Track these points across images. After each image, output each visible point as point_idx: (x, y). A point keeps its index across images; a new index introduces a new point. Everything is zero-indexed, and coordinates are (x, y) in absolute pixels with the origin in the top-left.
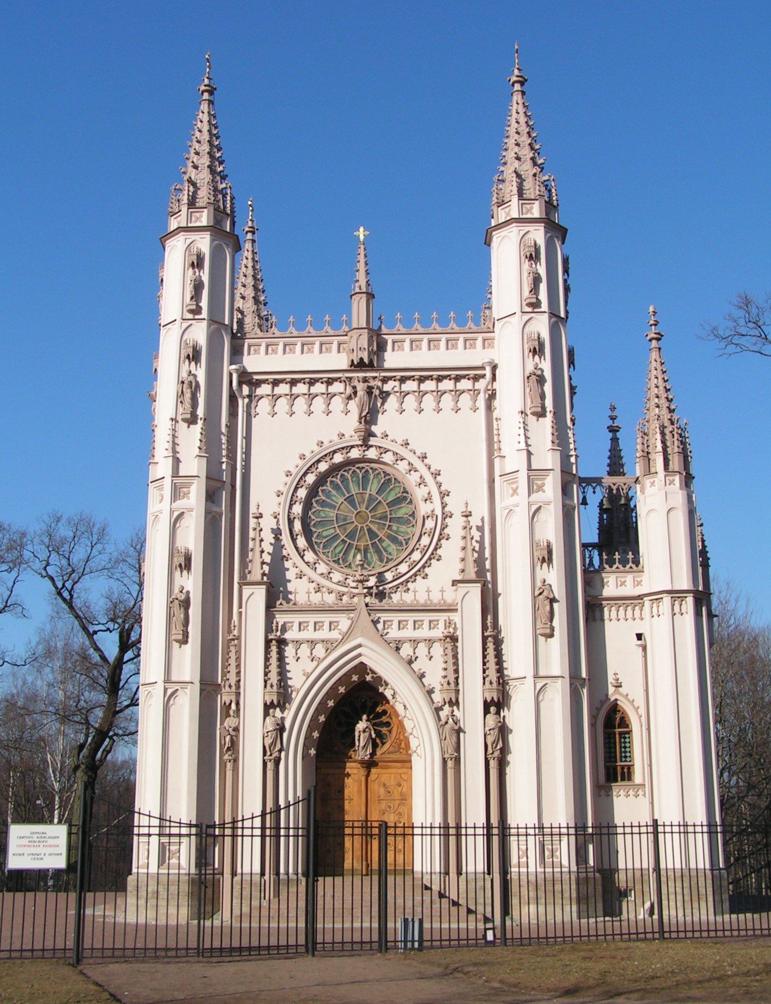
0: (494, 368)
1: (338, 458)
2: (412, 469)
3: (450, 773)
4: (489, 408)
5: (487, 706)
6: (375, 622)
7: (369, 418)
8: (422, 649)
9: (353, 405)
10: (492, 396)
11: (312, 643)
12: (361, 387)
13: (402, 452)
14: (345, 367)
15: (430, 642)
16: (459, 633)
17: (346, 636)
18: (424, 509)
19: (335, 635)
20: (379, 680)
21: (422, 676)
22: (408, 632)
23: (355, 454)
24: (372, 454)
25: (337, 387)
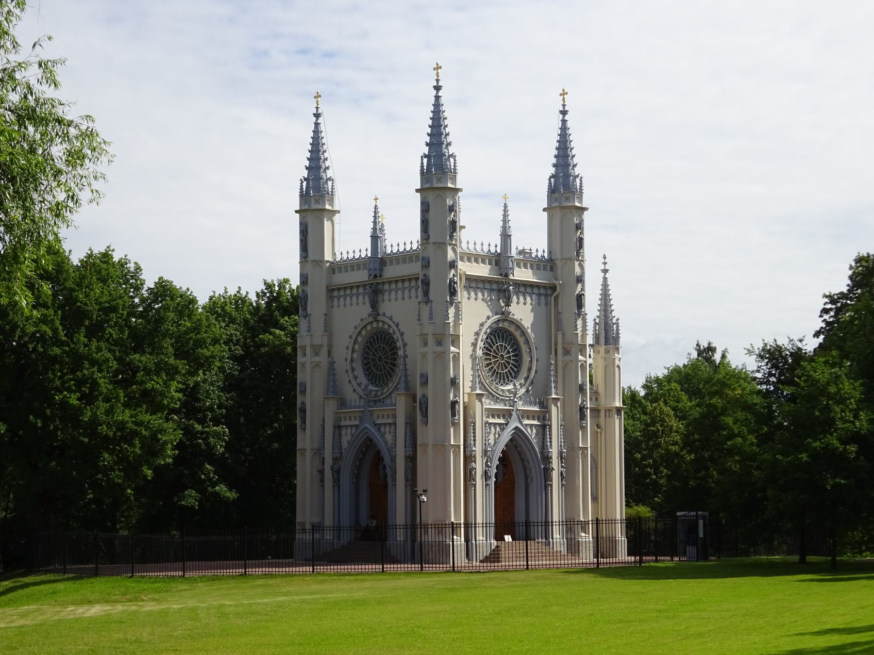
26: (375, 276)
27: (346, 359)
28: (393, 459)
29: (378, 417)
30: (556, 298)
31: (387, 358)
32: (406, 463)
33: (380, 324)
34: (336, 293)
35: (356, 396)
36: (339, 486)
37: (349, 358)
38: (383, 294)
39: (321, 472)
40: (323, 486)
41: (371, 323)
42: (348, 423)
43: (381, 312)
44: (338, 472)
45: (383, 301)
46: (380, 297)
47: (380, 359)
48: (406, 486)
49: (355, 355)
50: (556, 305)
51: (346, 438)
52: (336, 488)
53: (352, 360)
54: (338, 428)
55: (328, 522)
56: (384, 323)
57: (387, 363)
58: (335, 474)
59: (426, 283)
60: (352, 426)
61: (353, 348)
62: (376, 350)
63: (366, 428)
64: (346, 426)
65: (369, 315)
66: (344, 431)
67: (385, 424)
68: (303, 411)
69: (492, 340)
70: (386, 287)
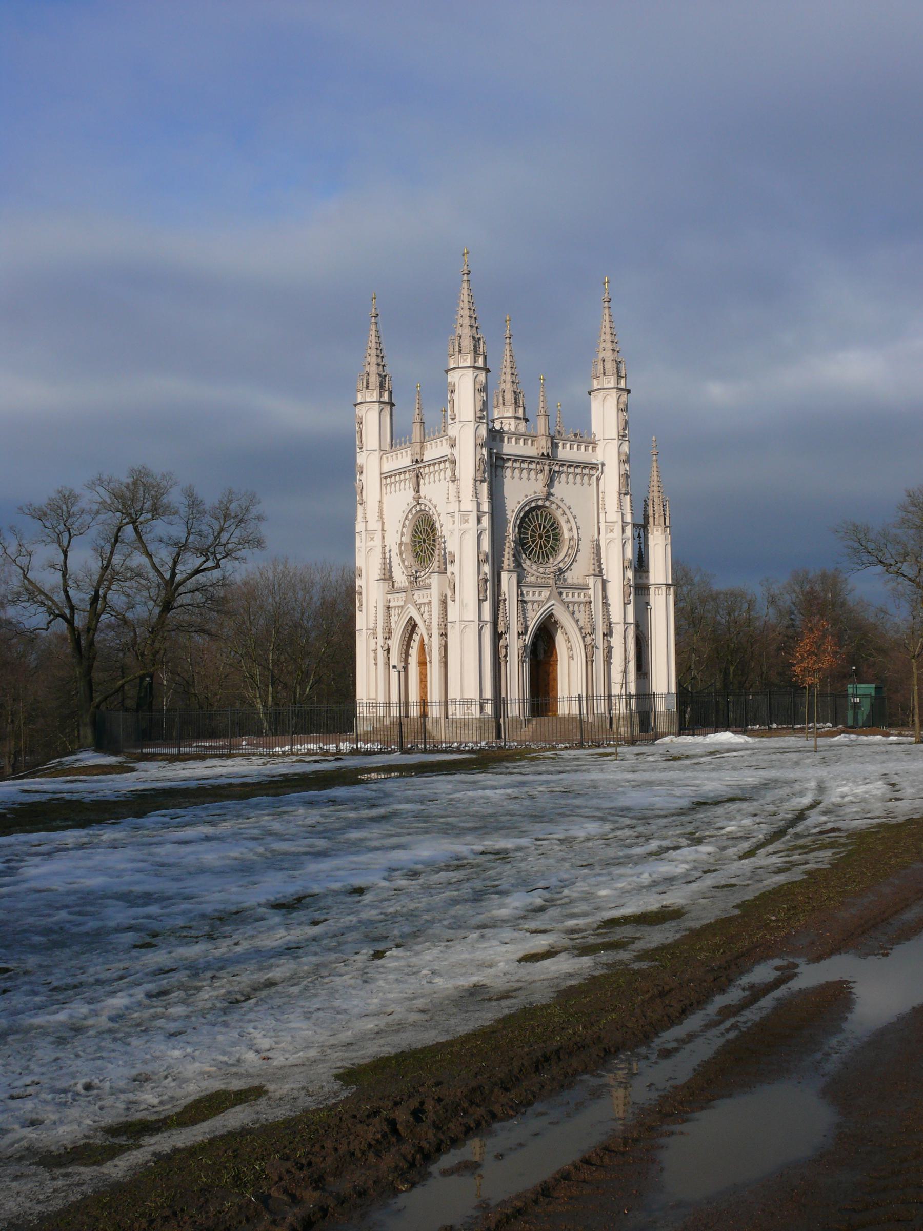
0: (603, 465)
1: (533, 504)
2: (564, 513)
3: (589, 667)
4: (598, 485)
5: (604, 635)
6: (561, 594)
7: (550, 484)
8: (576, 608)
9: (540, 476)
10: (598, 479)
11: (533, 602)
12: (547, 468)
13: (560, 504)
14: (536, 455)
15: (580, 603)
16: (592, 599)
17: (548, 599)
18: (566, 535)
19: (542, 598)
20: (556, 622)
21: (577, 621)
22: (570, 598)
23: (540, 503)
24: (547, 504)
25: (533, 466)
26: (417, 461)
31: (429, 540)
39: (375, 651)
40: (376, 664)
43: (422, 494)
44: (388, 650)
46: (422, 482)
49: (403, 539)
50: (598, 485)
51: (393, 619)
53: (400, 544)
55: (381, 699)
56: (426, 505)
59: (454, 462)
68: (361, 594)
69: (529, 520)
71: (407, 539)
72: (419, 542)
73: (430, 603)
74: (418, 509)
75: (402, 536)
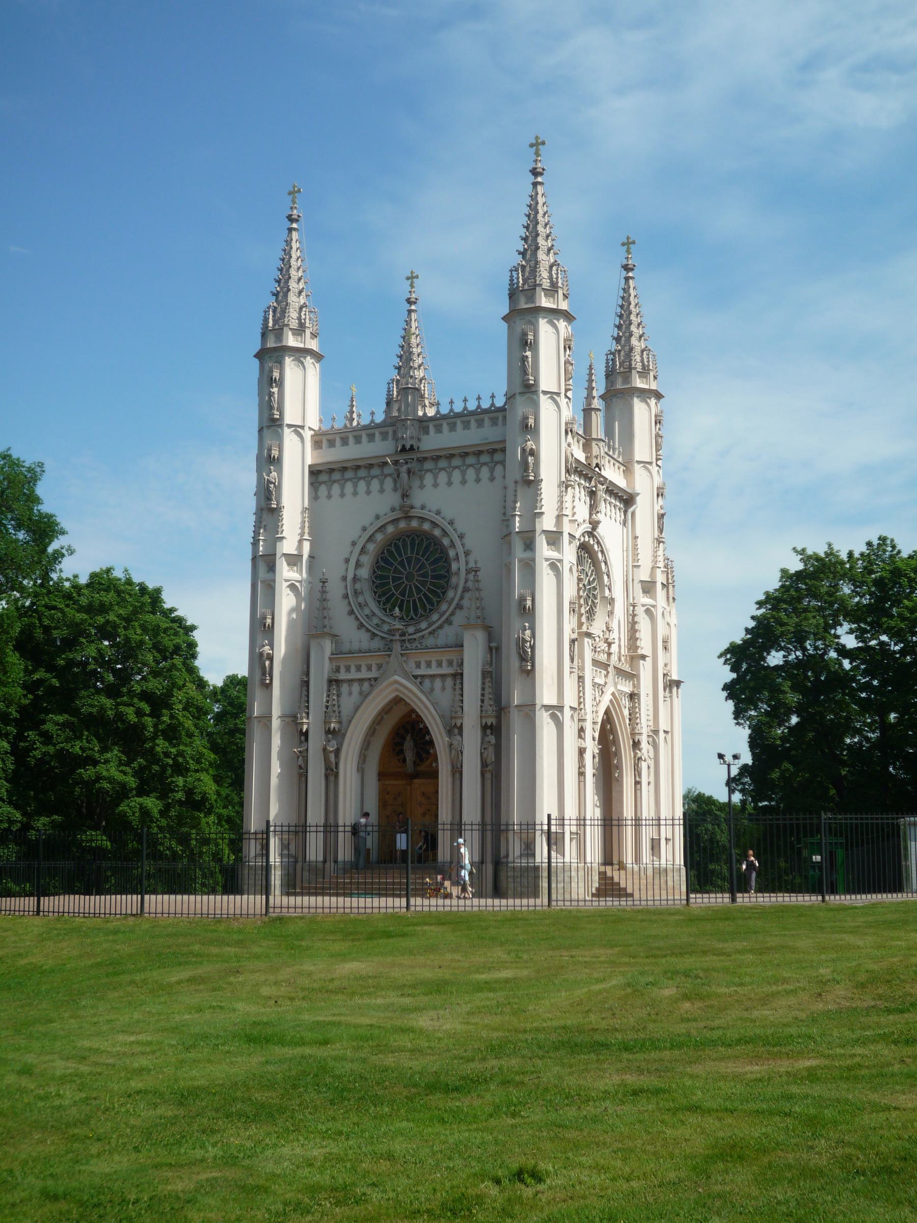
27: (344, 579)
28: (455, 729)
29: (418, 665)
30: (633, 514)
32: (484, 735)
33: (414, 524)
34: (323, 477)
35: (364, 636)
36: (336, 775)
37: (350, 576)
38: (422, 478)
41: (395, 521)
42: (353, 675)
44: (337, 752)
45: (422, 487)
46: (416, 483)
47: (409, 577)
48: (483, 774)
52: (332, 778)
53: (355, 579)
54: (334, 683)
57: (423, 583)
58: (332, 757)
60: (361, 680)
61: (358, 561)
62: (401, 563)
63: (396, 682)
64: (350, 681)
65: (393, 510)
66: (345, 688)
67: (433, 677)
70: (428, 465)
71: (364, 573)
72: (395, 579)
73: (458, 676)
74: (402, 525)
75: (358, 565)
